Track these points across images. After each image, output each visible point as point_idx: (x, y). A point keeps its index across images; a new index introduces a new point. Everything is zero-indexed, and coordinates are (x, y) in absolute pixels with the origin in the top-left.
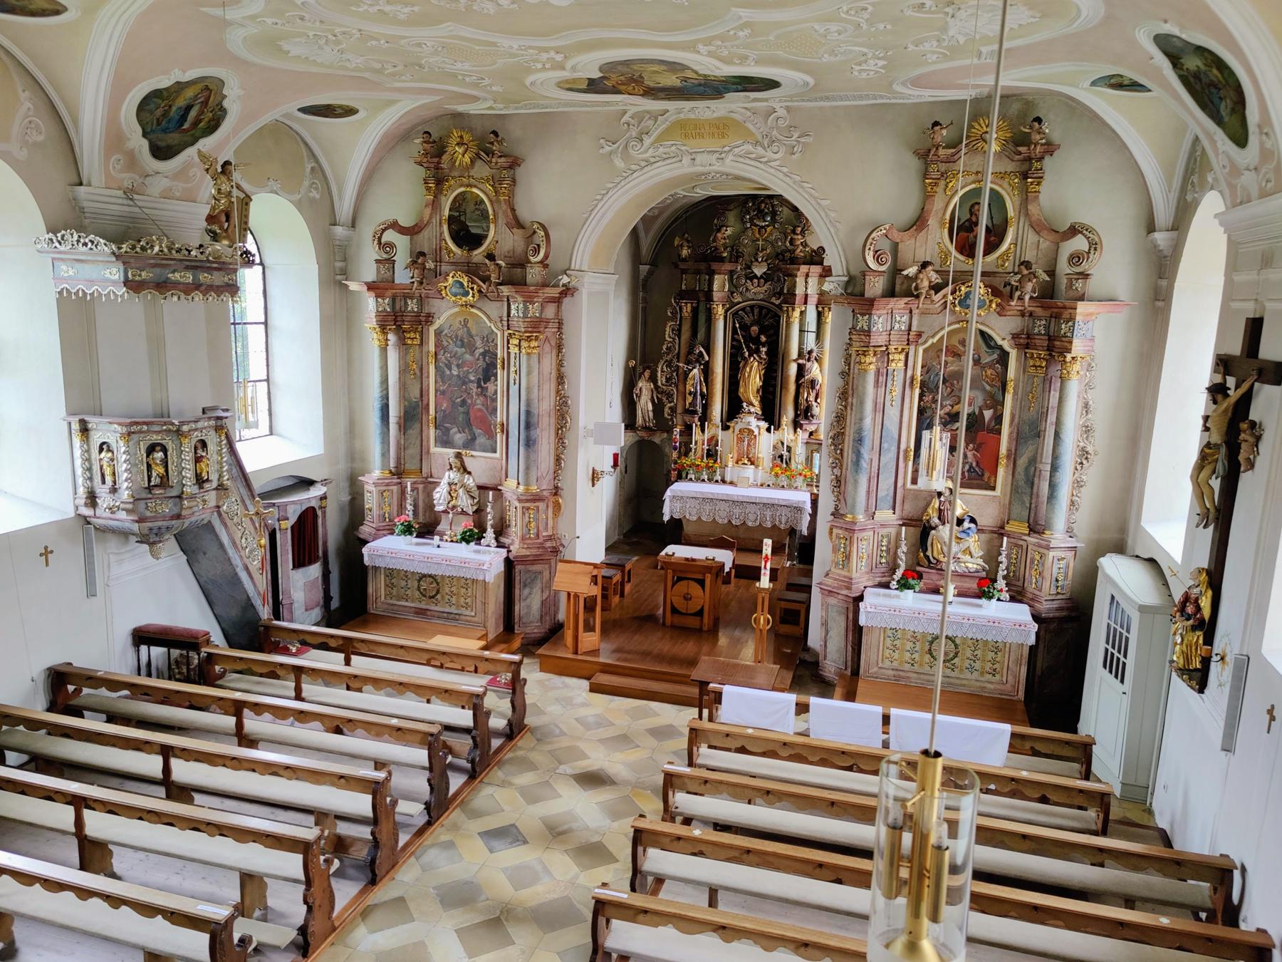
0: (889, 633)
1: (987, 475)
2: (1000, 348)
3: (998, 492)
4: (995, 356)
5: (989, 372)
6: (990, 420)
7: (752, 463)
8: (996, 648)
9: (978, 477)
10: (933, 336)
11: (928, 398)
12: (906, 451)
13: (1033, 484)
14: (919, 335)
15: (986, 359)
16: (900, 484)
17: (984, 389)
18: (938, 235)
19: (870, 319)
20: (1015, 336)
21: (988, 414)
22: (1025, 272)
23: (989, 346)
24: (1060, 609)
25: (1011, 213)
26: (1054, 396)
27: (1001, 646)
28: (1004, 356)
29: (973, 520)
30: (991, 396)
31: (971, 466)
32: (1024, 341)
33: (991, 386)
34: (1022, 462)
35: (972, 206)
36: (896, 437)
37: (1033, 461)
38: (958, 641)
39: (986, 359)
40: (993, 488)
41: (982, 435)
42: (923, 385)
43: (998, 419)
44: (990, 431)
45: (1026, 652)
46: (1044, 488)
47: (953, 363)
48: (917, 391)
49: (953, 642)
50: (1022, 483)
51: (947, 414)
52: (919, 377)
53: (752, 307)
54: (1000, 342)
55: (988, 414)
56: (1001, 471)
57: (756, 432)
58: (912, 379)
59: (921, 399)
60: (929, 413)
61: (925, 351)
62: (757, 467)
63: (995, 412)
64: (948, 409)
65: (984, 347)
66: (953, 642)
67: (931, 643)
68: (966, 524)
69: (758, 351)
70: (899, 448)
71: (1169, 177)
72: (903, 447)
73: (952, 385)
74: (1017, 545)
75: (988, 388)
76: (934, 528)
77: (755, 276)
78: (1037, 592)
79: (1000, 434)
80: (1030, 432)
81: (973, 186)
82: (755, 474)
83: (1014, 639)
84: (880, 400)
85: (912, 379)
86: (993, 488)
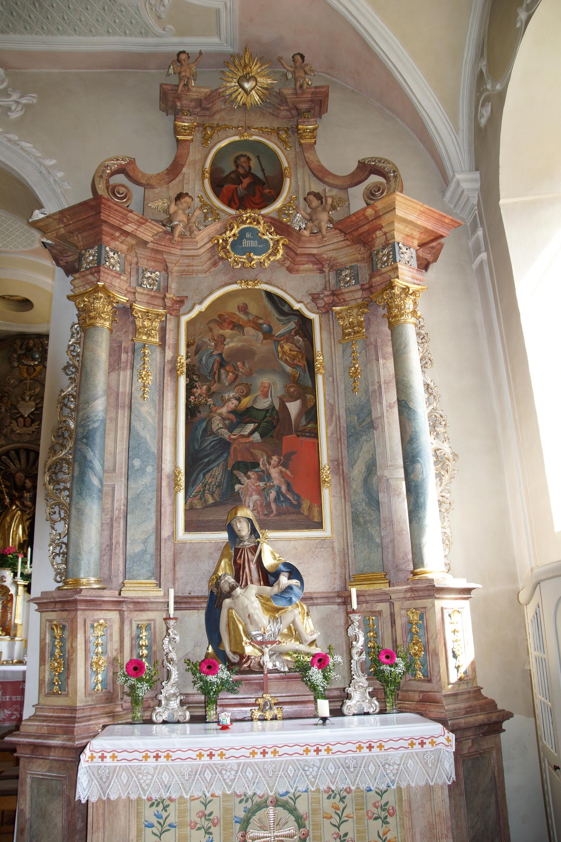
0: (149, 814)
1: (306, 504)
2: (298, 314)
3: (326, 532)
4: (292, 325)
5: (287, 347)
6: (299, 415)
7: (8, 634)
8: (385, 813)
9: (297, 511)
10: (201, 303)
11: (201, 390)
12: (175, 475)
13: (378, 503)
14: (181, 301)
15: (281, 330)
16: (166, 533)
17: (283, 372)
18: (198, 187)
19: (99, 253)
20: (315, 298)
21: (294, 407)
22: (315, 203)
23: (281, 312)
24: (470, 711)
25: (285, 164)
26: (387, 368)
27: (390, 798)
28: (305, 326)
29: (294, 573)
30: (295, 381)
31: (279, 492)
32: (329, 301)
33: (294, 366)
34: (357, 472)
35: (238, 158)
36: (154, 449)
37: (371, 468)
38: (302, 807)
39: (281, 330)
40: (319, 525)
41: (289, 440)
42: (191, 372)
43: (311, 413)
44: (301, 433)
45: (442, 802)
46: (402, 506)
47: (232, 337)
48: (183, 381)
49: (292, 811)
50: (362, 507)
51: (233, 412)
52: (183, 359)
53: (17, 451)
54: (297, 306)
55: (294, 407)
56: (326, 493)
57: (12, 591)
58: (174, 360)
59: (190, 389)
60: (203, 414)
61: (190, 323)
62: (13, 639)
63: (304, 403)
64: (232, 404)
65: (275, 315)
66: (292, 811)
67: (245, 823)
68: (284, 580)
69: (21, 498)
70: (160, 469)
71: (453, 117)
72: (167, 467)
73: (235, 368)
74: (373, 613)
75: (288, 369)
76: (229, 595)
77: (22, 416)
78: (426, 687)
79: (315, 435)
80: (360, 425)
81: (237, 138)
82: (11, 648)
83: (415, 778)
84: (124, 389)
85: (174, 360)
86: (319, 525)
